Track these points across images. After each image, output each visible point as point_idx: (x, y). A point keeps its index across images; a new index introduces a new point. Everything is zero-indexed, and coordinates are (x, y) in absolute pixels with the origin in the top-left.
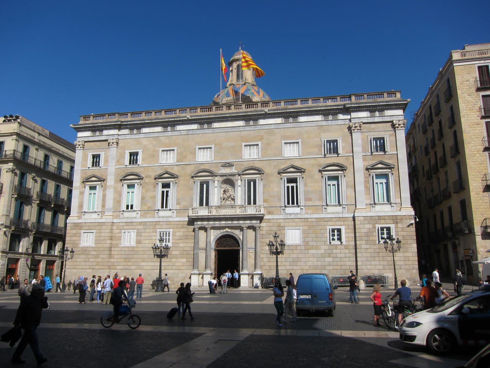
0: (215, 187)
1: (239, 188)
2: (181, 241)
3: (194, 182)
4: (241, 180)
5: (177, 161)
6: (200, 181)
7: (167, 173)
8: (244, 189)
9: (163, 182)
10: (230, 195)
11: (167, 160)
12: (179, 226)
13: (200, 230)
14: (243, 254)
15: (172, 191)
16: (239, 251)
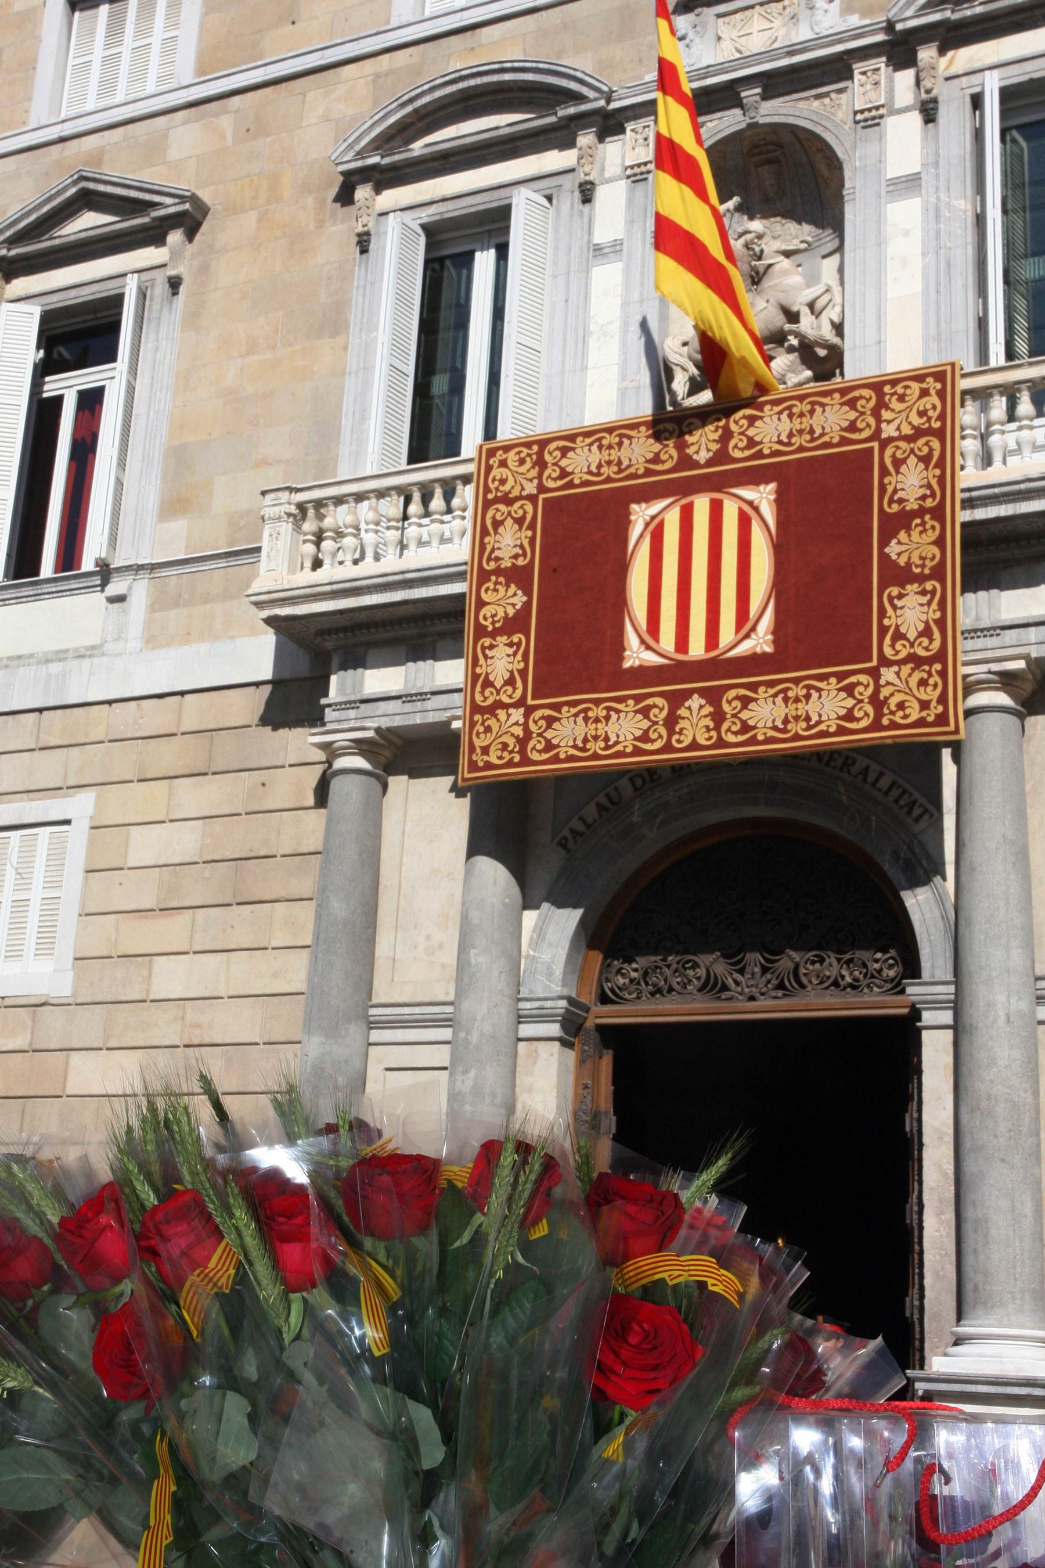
0: (598, 249)
1: (905, 215)
2: (174, 931)
3: (363, 243)
4: (929, 112)
5: (201, 70)
6: (426, 215)
7: (87, 199)
8: (964, 205)
9: (56, 302)
10: (779, 320)
11: (107, 85)
12: (167, 756)
13: (398, 783)
14: (965, 1082)
15: (139, 389)
16: (901, 1037)
